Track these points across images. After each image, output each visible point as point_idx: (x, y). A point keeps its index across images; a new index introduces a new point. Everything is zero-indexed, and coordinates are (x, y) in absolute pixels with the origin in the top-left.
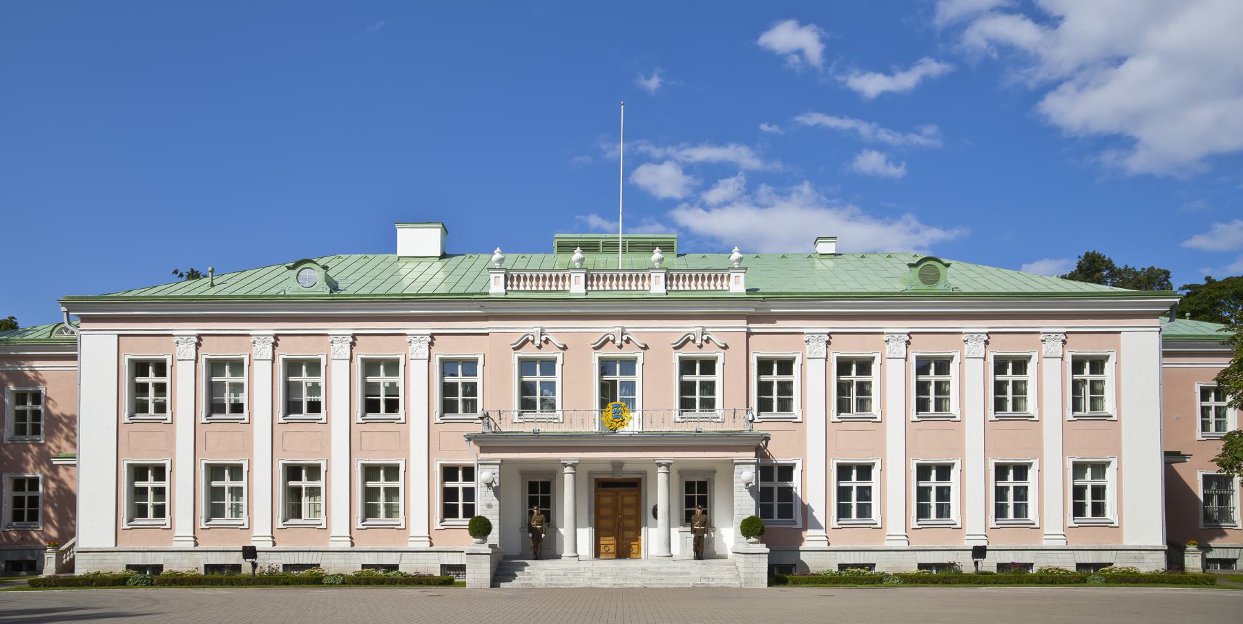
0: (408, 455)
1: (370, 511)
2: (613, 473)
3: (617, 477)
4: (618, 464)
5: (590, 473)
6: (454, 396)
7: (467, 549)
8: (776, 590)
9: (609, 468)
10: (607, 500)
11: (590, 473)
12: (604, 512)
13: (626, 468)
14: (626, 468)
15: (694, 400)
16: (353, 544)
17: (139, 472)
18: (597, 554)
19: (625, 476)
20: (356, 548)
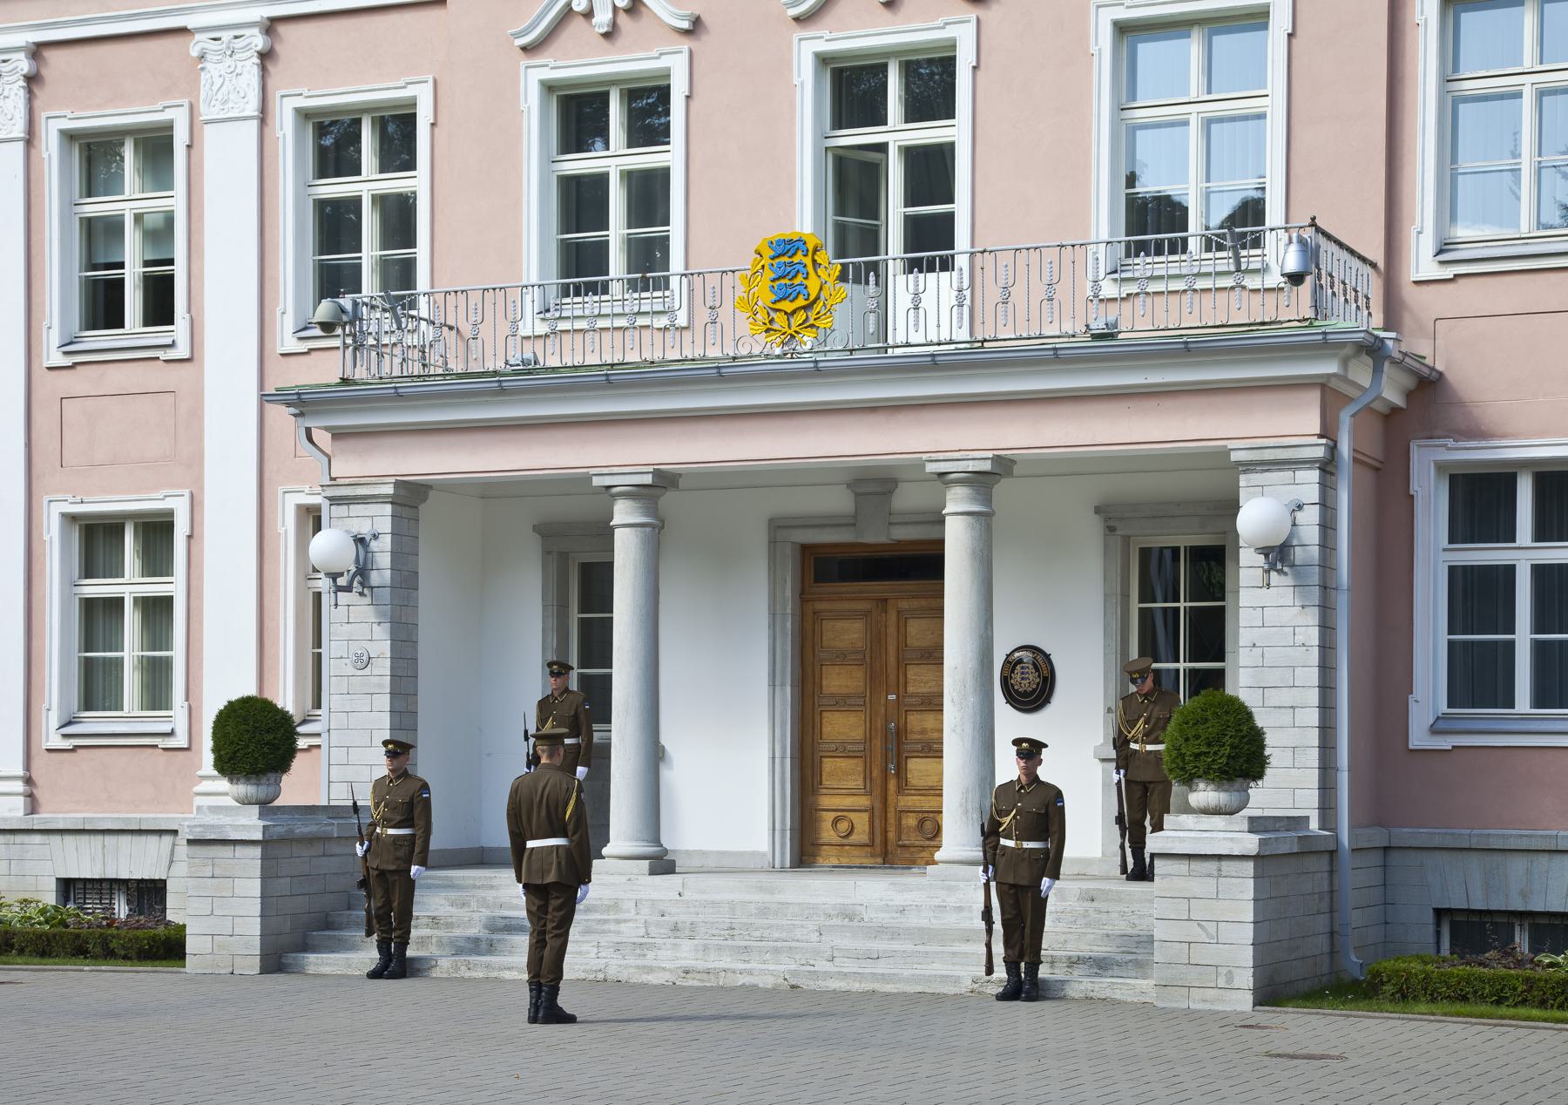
0: (199, 480)
1: (96, 687)
2: (851, 522)
3: (875, 535)
4: (873, 484)
5: (778, 526)
6: (350, 249)
7: (189, 821)
8: (1268, 1015)
9: (839, 502)
10: (847, 633)
11: (778, 526)
12: (837, 681)
13: (907, 499)
14: (907, 499)
15: (603, 246)
16: (33, 805)
17: (97, 539)
18: (805, 850)
19: (902, 534)
20: (48, 817)
